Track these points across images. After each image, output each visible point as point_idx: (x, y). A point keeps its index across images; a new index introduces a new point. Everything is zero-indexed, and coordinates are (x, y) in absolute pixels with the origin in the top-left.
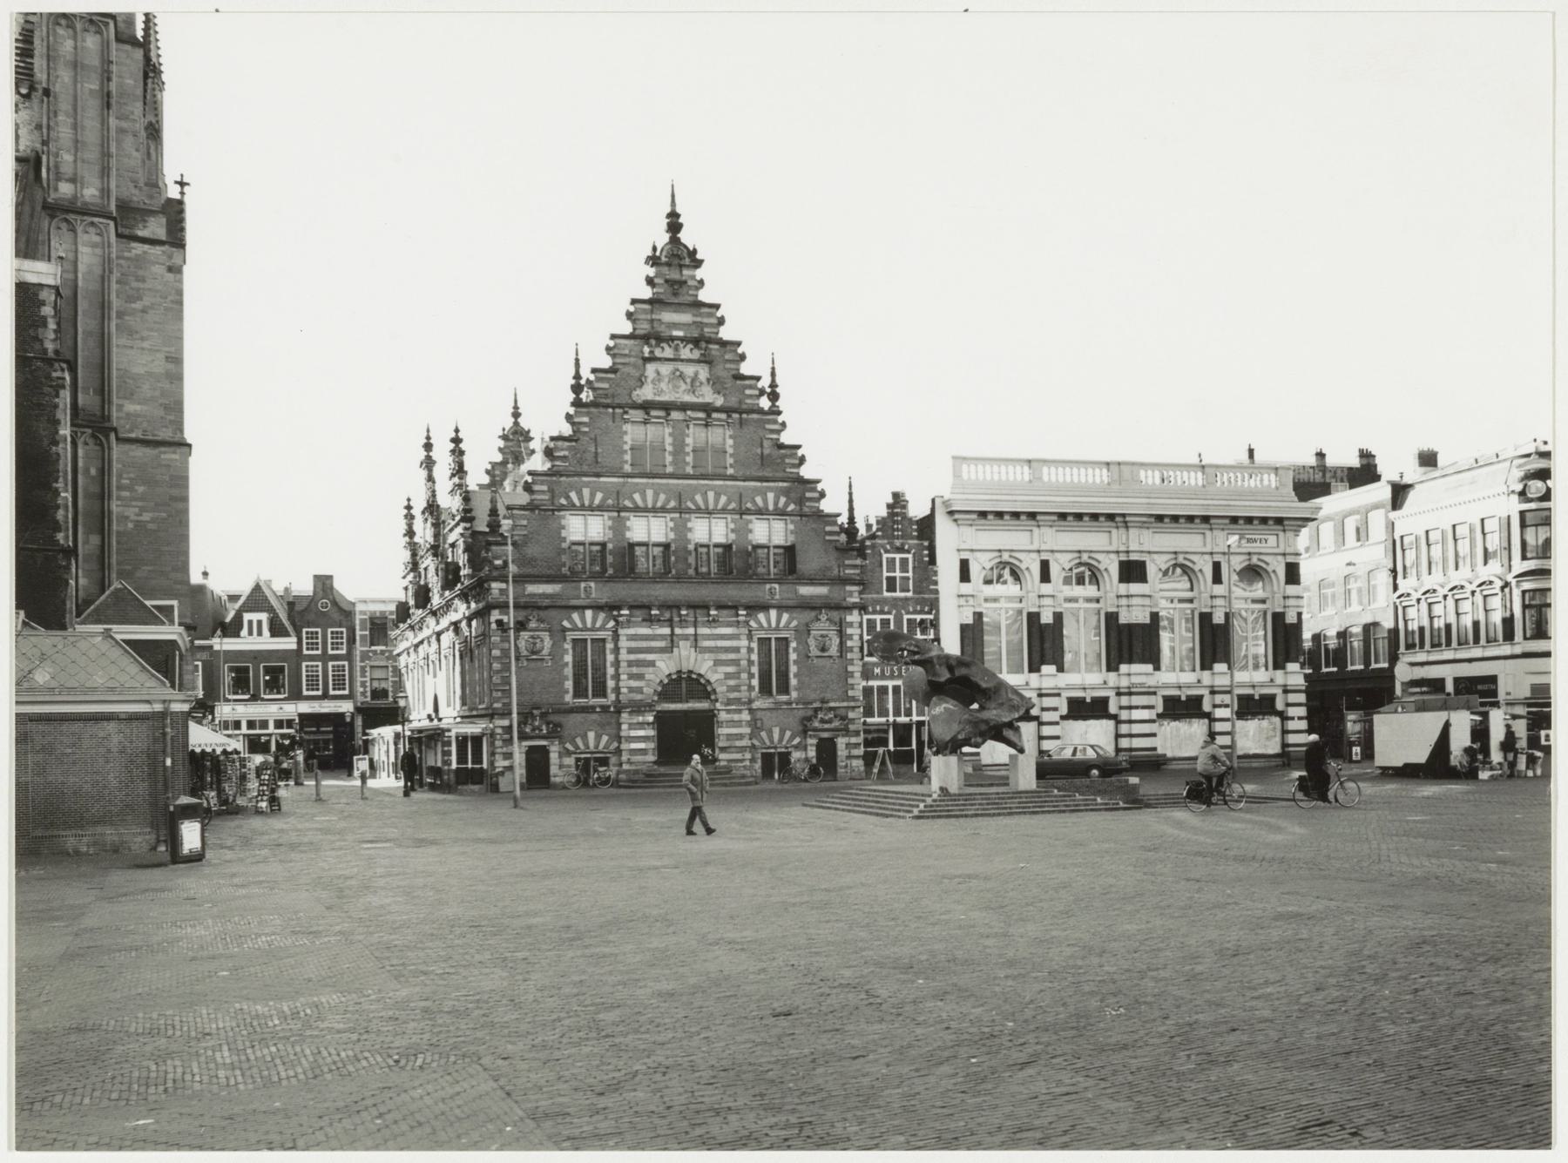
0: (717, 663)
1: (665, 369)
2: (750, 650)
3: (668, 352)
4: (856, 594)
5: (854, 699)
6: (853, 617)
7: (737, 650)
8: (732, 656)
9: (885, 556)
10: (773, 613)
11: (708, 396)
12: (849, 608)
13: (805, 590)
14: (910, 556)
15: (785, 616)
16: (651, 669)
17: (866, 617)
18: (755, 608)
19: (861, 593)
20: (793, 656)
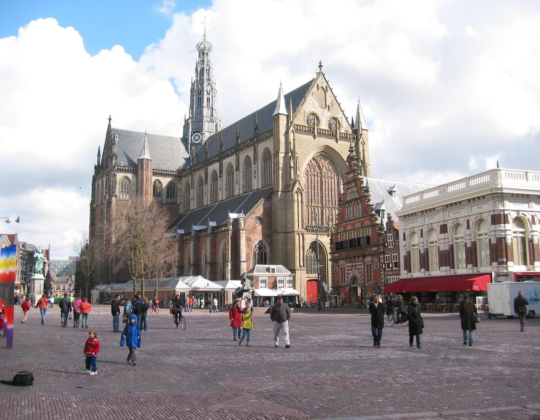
0: (360, 273)
1: (350, 190)
2: (364, 268)
3: (350, 186)
4: (382, 249)
5: (382, 283)
6: (382, 257)
7: (361, 269)
8: (360, 271)
9: (388, 235)
10: (368, 257)
11: (357, 196)
12: (380, 254)
13: (374, 249)
14: (392, 234)
15: (370, 257)
16: (349, 275)
17: (385, 256)
18: (364, 256)
19: (383, 248)
20: (372, 270)
